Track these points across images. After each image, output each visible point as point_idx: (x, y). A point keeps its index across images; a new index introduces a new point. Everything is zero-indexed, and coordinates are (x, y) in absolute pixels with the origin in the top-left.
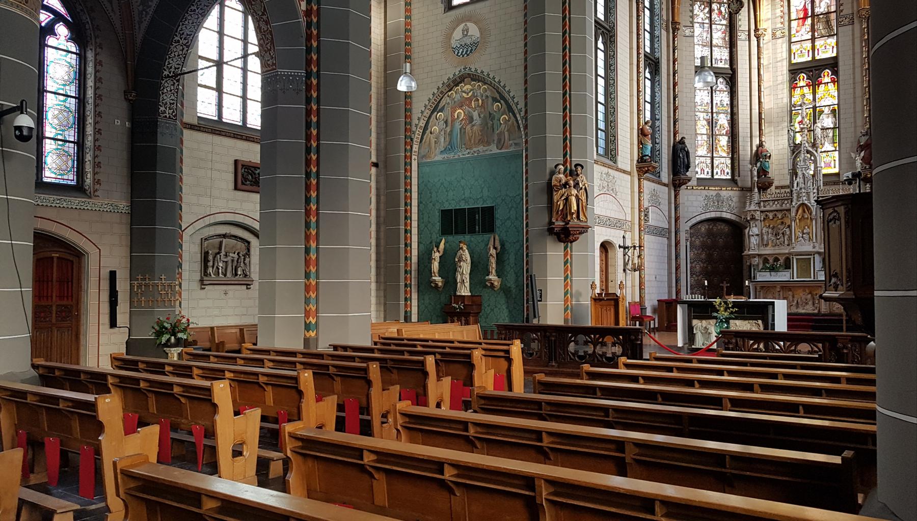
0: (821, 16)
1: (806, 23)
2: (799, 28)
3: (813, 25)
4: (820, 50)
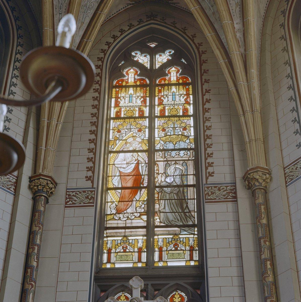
0: (168, 190)
1: (137, 197)
2: (122, 205)
3: (150, 202)
4: (164, 249)
